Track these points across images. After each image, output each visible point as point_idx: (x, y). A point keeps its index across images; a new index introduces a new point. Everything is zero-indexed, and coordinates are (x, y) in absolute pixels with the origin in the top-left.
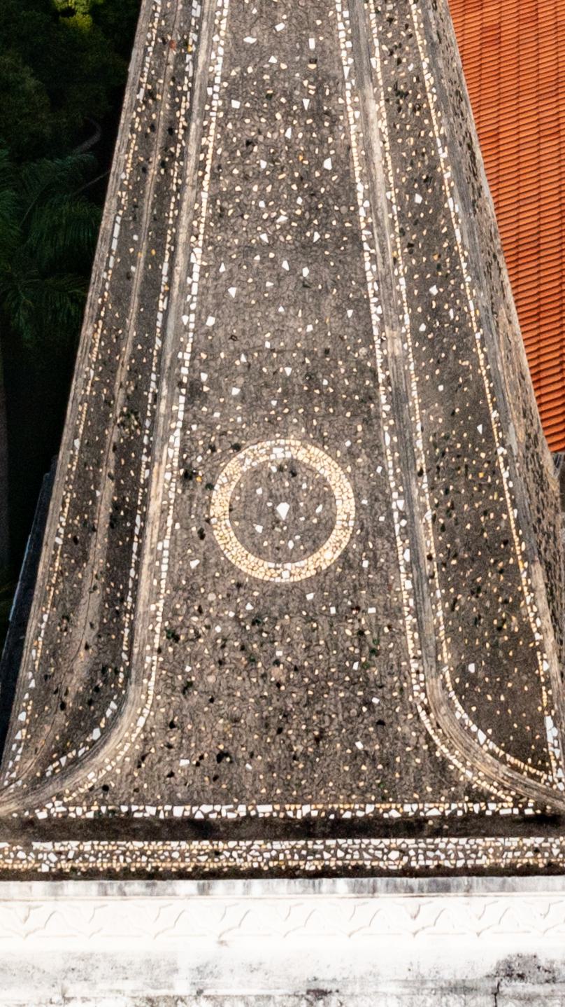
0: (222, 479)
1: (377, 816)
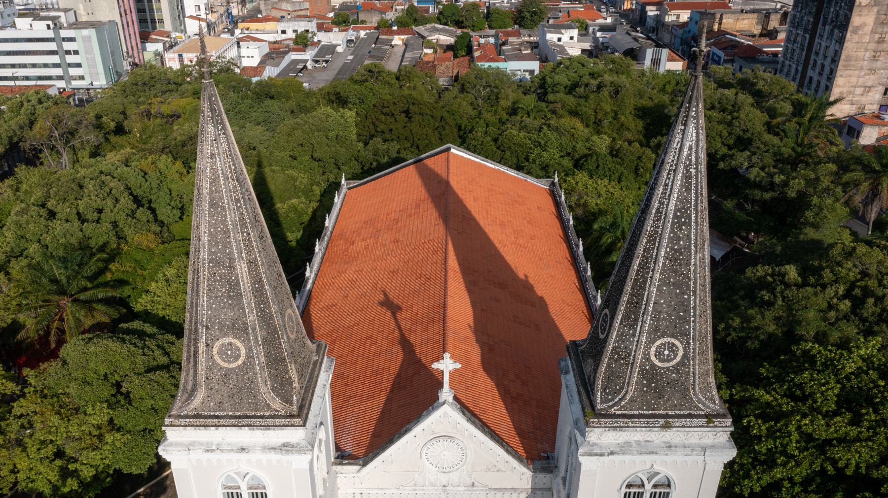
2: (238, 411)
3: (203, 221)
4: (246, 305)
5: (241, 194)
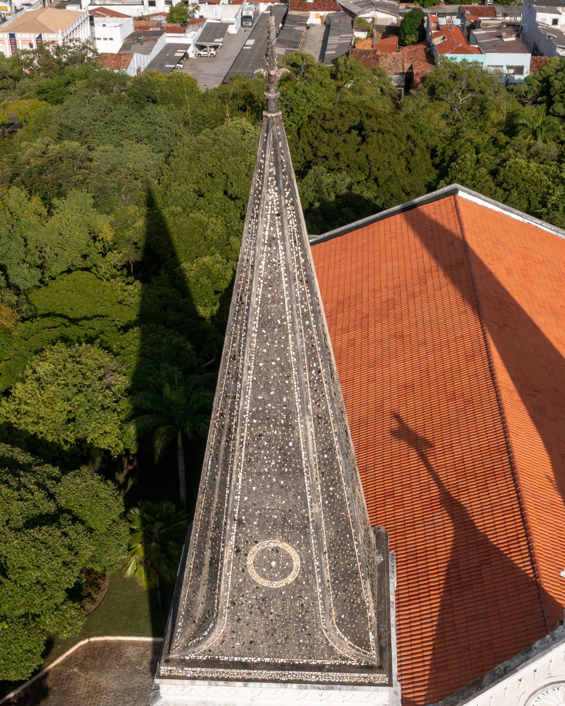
0: (251, 552)
1: (308, 664)
2: (280, 657)
3: (248, 349)
4: (307, 489)
5: (312, 304)
